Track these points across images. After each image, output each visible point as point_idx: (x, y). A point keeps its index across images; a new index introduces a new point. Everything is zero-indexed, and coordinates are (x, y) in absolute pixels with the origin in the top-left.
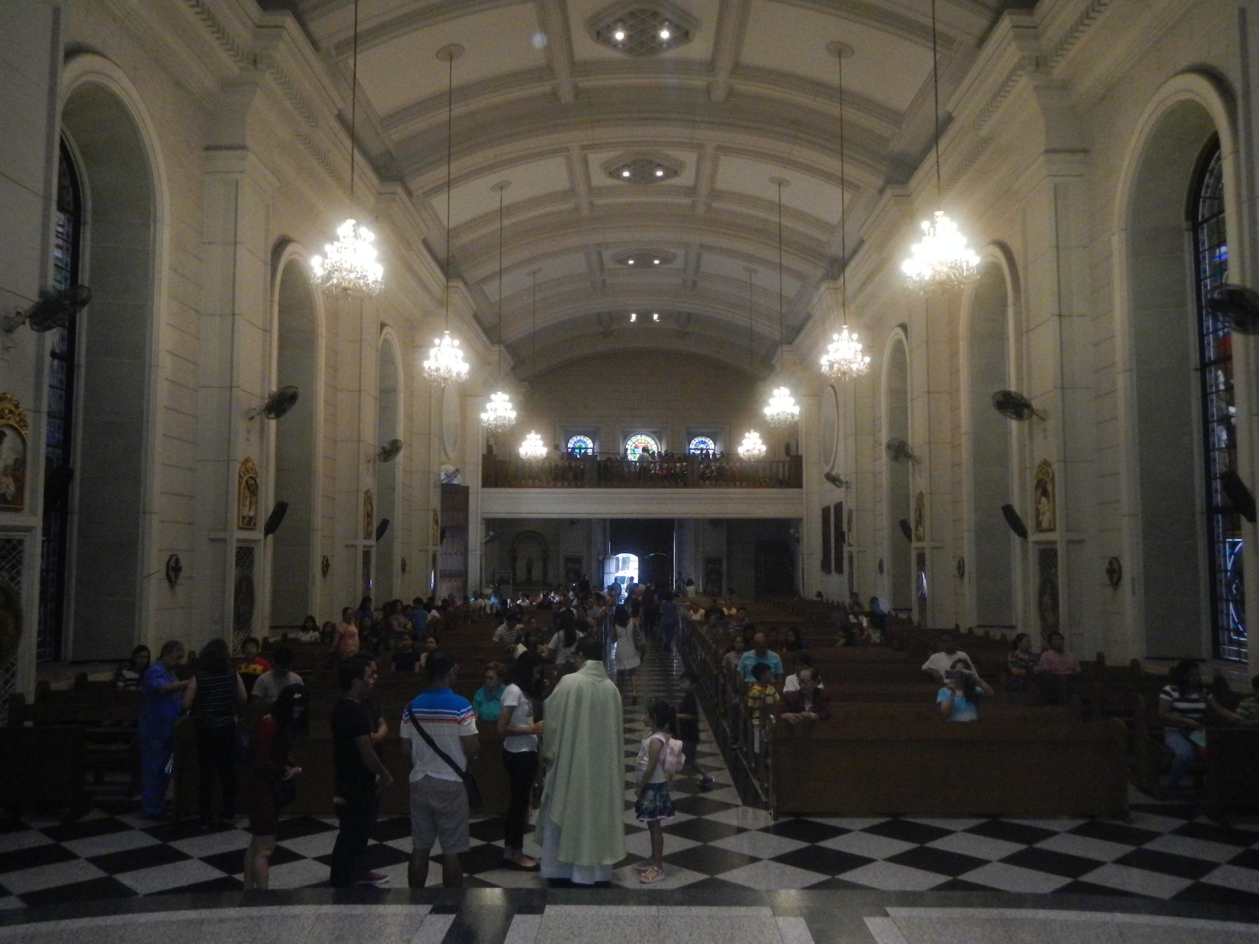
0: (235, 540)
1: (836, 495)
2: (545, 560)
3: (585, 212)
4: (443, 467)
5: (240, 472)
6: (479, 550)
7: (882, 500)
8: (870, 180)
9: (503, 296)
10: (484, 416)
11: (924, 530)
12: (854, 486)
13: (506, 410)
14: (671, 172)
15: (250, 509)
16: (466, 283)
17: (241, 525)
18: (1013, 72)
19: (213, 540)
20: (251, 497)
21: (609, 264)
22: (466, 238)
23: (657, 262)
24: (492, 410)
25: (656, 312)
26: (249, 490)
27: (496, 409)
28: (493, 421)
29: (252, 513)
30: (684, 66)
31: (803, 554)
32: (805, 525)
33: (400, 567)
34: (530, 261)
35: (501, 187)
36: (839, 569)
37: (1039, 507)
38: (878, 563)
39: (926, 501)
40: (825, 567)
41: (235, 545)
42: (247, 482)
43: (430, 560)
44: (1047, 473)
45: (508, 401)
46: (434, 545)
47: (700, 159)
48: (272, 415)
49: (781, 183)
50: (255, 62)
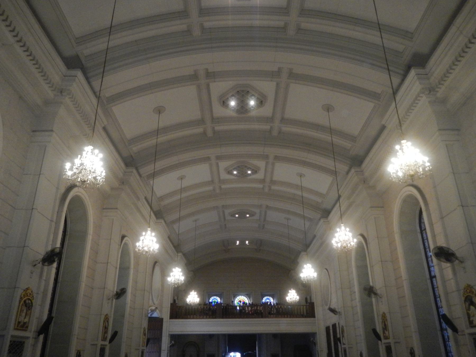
0: (9, 336)
1: (333, 319)
3: (218, 191)
5: (21, 295)
6: (166, 350)
7: (359, 320)
8: (342, 167)
11: (389, 333)
13: (179, 276)
14: (255, 172)
15: (25, 318)
16: (165, 222)
17: (16, 327)
18: (418, 96)
20: (27, 311)
21: (228, 218)
22: (167, 202)
23: (248, 216)
24: (173, 276)
25: (248, 240)
26: (26, 306)
27: (175, 275)
28: (174, 281)
29: (26, 320)
30: (260, 119)
31: (318, 351)
35: (182, 178)
37: (470, 312)
38: (359, 354)
39: (388, 318)
42: (25, 301)
44: (471, 292)
45: (181, 272)
46: (143, 346)
47: (267, 163)
48: (46, 264)
49: (301, 175)
50: (61, 92)
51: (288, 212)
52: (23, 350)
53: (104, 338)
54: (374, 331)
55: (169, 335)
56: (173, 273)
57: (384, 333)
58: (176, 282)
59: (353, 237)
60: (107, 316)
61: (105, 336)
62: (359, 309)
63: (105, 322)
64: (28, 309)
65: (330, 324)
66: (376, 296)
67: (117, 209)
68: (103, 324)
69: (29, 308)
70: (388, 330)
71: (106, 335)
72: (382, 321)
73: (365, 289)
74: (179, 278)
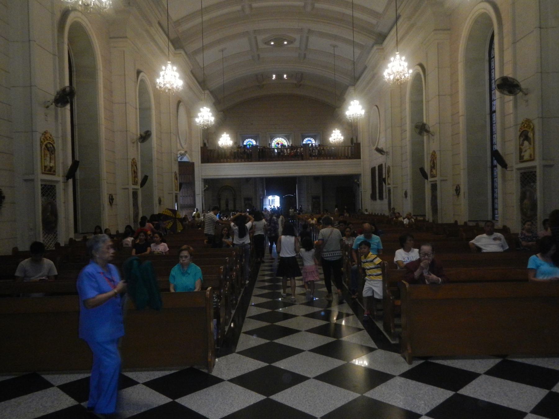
0: (39, 180)
1: (379, 159)
2: (235, 200)
4: (179, 152)
5: (41, 139)
7: (407, 160)
10: (197, 120)
11: (436, 172)
12: (391, 154)
13: (209, 116)
15: (50, 162)
16: (186, 53)
17: (43, 171)
19: (26, 180)
20: (50, 155)
21: (262, 46)
22: (186, 26)
23: (286, 43)
24: (201, 116)
26: (49, 150)
27: (203, 116)
28: (203, 122)
29: (52, 164)
31: (361, 192)
33: (157, 202)
34: (219, 42)
36: (381, 198)
37: (522, 147)
38: (404, 192)
40: (373, 197)
41: (40, 183)
42: (46, 145)
44: (529, 126)
45: (210, 112)
46: (176, 190)
48: (59, 105)
51: (335, 37)
52: (55, 194)
53: (134, 181)
54: (422, 170)
55: (202, 179)
57: (431, 171)
58: (205, 124)
59: (409, 68)
60: (134, 161)
61: (136, 181)
62: (408, 149)
63: (133, 167)
65: (376, 164)
66: (428, 133)
67: (126, 37)
68: (132, 169)
71: (136, 179)
72: (431, 160)
73: (417, 127)
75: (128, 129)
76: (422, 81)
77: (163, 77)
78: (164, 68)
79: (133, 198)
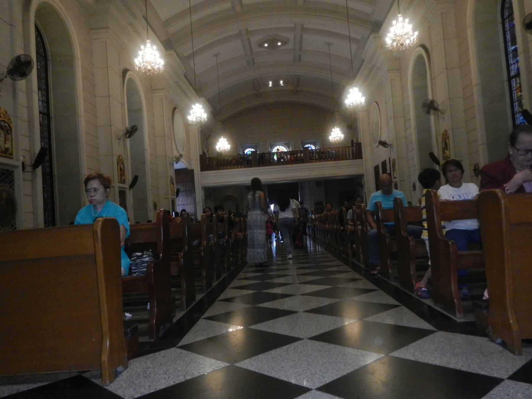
1: (383, 154)
6: (201, 203)
7: (413, 150)
9: (195, 50)
11: (450, 152)
12: (395, 146)
21: (256, 49)
31: (365, 192)
32: (365, 177)
43: (171, 203)
45: (202, 109)
51: (330, 34)
53: (121, 180)
54: (432, 155)
56: (193, 110)
57: (444, 152)
58: (198, 121)
59: (414, 30)
60: (121, 157)
61: (123, 179)
62: (414, 137)
63: (119, 165)
64: (6, 134)
65: (379, 162)
66: (436, 112)
67: (108, 28)
68: (118, 165)
69: (7, 131)
70: (449, 148)
71: (123, 177)
72: (443, 141)
73: (424, 105)
74: (200, 116)
75: (112, 124)
76: (424, 64)
77: (141, 57)
78: (142, 47)
79: (119, 197)
